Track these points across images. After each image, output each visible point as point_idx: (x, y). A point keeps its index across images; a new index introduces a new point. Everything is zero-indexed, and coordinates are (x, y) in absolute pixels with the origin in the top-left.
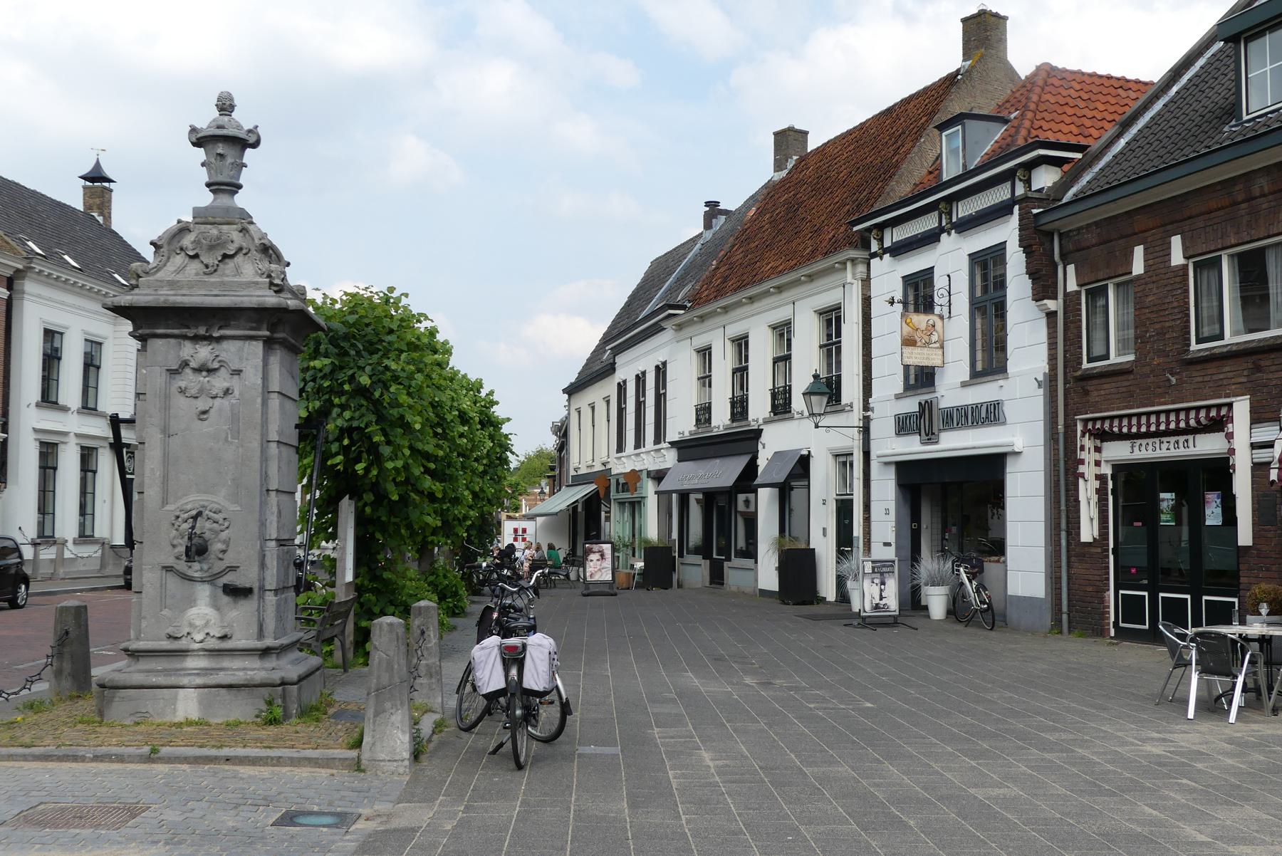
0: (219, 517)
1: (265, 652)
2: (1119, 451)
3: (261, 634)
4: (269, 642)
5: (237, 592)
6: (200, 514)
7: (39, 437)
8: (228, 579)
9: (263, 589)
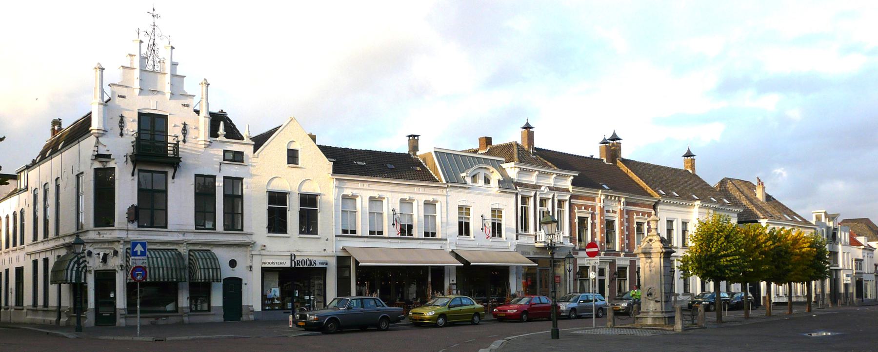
1: (662, 312)
3: (662, 309)
4: (664, 310)
5: (657, 302)
8: (657, 299)
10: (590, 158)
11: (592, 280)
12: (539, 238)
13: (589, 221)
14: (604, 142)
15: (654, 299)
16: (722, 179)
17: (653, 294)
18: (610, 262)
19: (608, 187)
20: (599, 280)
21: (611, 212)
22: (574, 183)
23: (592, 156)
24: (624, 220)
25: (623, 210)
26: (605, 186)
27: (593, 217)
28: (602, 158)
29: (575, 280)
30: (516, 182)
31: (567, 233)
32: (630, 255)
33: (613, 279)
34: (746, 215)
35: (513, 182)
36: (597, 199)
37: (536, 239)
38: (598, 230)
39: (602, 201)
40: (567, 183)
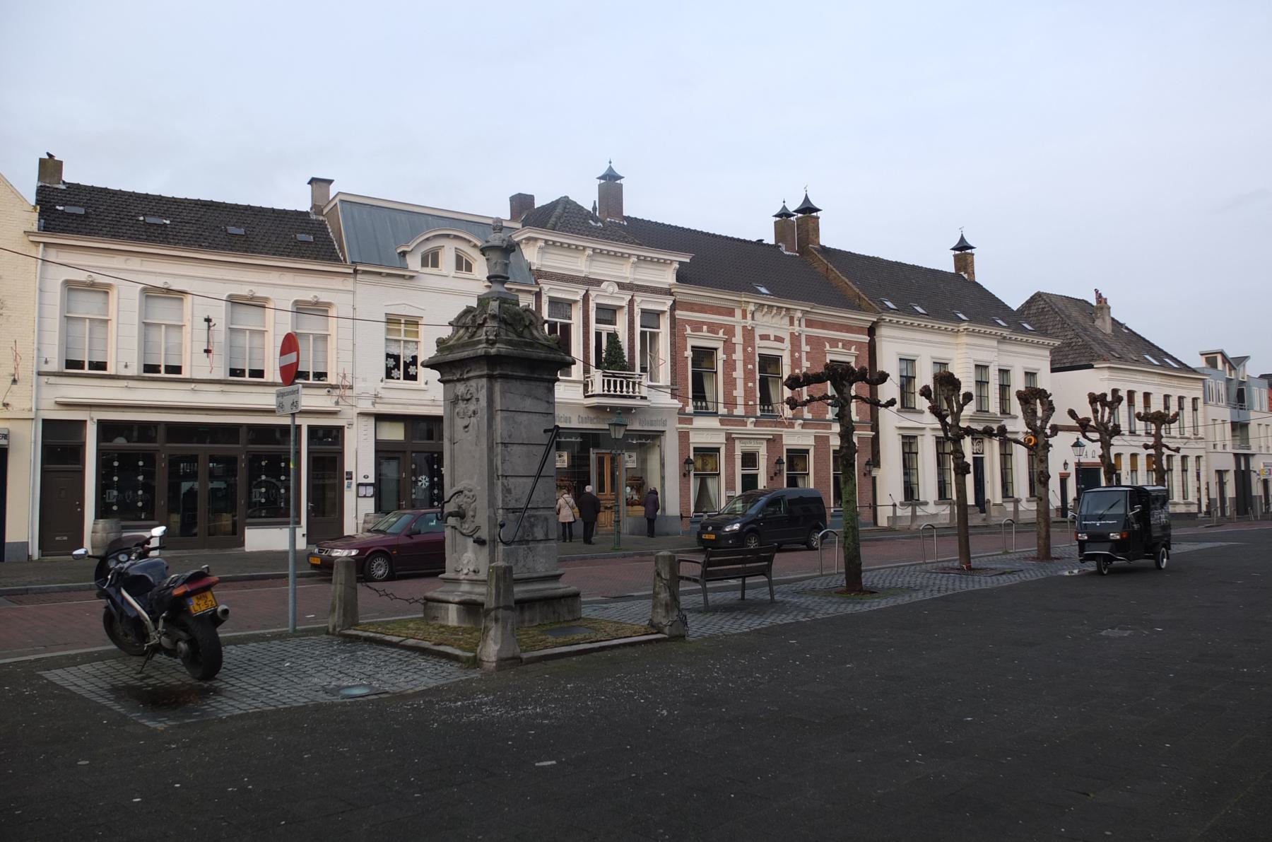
7: (900, 433)
12: (592, 388)
13: (721, 356)
14: (784, 215)
16: (1033, 294)
18: (768, 440)
20: (743, 476)
21: (772, 338)
22: (682, 277)
24: (800, 357)
25: (800, 334)
26: (763, 290)
27: (729, 347)
29: (684, 475)
30: (538, 270)
31: (664, 377)
33: (776, 474)
34: (1072, 356)
35: (530, 269)
36: (738, 313)
37: (586, 390)
38: (739, 374)
39: (749, 316)
40: (667, 277)
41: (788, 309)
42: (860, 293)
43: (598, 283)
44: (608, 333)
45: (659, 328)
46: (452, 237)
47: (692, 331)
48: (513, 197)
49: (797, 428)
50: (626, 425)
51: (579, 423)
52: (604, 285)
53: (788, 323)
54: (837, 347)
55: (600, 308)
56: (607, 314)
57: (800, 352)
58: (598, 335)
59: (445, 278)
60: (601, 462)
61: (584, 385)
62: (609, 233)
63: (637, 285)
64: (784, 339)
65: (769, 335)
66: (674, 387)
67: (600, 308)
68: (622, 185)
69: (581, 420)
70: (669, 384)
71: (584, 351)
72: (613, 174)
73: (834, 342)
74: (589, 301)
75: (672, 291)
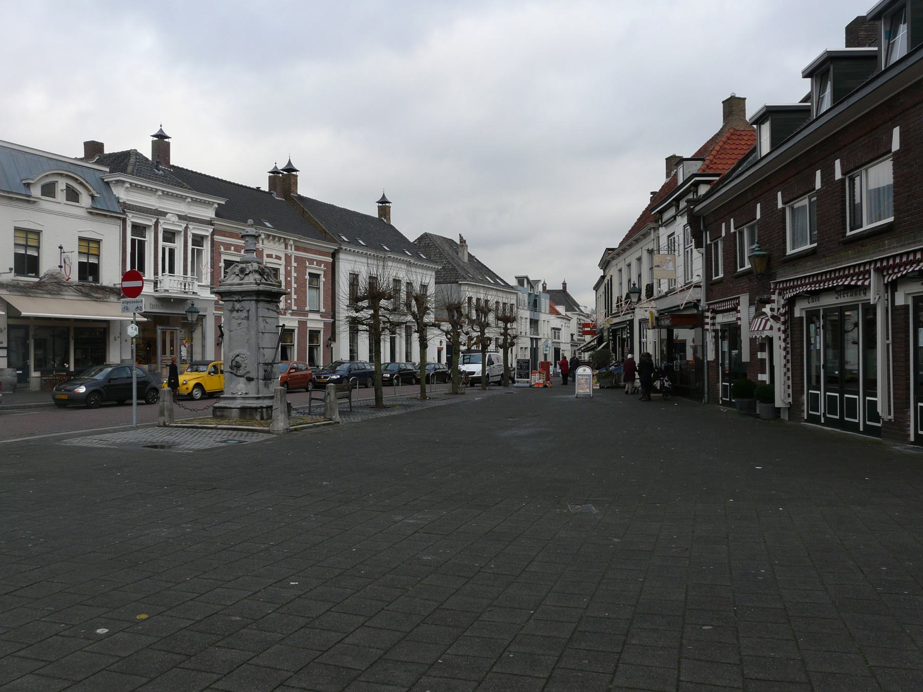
0: (244, 356)
2: (720, 319)
5: (250, 380)
6: (238, 355)
8: (248, 375)
9: (257, 378)
10: (257, 190)
11: (132, 338)
14: (275, 172)
15: (246, 374)
17: (243, 365)
19: (272, 225)
21: (274, 257)
23: (259, 188)
24: (291, 270)
26: (268, 224)
28: (272, 192)
29: (218, 344)
30: (124, 203)
31: (206, 280)
32: (299, 315)
35: (118, 202)
40: (209, 214)
41: (285, 239)
42: (326, 229)
43: (164, 214)
44: (169, 249)
45: (203, 247)
46: (64, 175)
47: (224, 250)
48: (86, 142)
49: (288, 316)
50: (199, 312)
51: (151, 308)
52: (168, 216)
53: (284, 247)
54: (313, 264)
55: (166, 231)
56: (170, 236)
57: (291, 267)
58: (164, 249)
59: (59, 204)
60: (164, 333)
61: (154, 283)
62: (169, 179)
63: (190, 217)
64: (281, 258)
65: (272, 255)
66: (213, 286)
67: (166, 231)
68: (169, 143)
69: (152, 306)
70: (209, 284)
71: (154, 260)
72: (164, 134)
73: (311, 261)
74: (158, 226)
75: (213, 222)
